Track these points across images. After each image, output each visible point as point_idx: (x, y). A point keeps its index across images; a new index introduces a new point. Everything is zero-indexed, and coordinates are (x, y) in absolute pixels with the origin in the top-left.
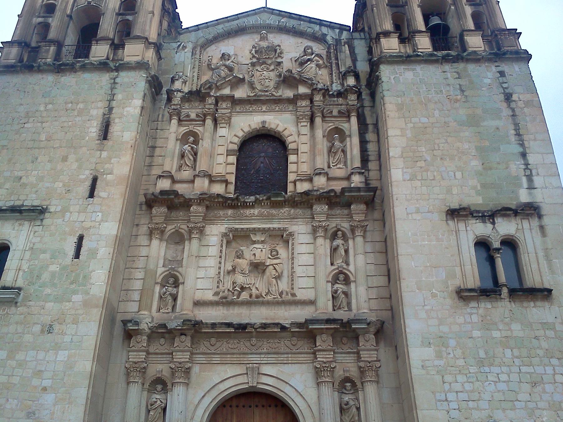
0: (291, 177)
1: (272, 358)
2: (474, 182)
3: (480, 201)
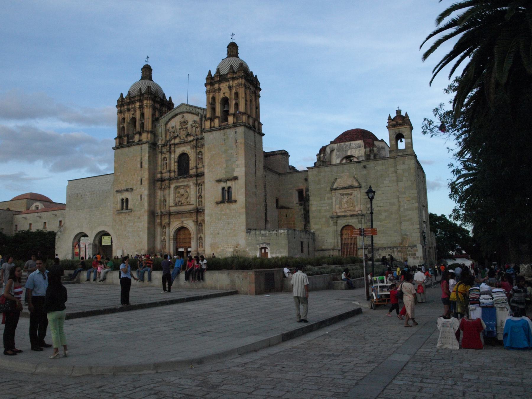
0: (190, 168)
1: (185, 219)
2: (224, 171)
3: (224, 176)
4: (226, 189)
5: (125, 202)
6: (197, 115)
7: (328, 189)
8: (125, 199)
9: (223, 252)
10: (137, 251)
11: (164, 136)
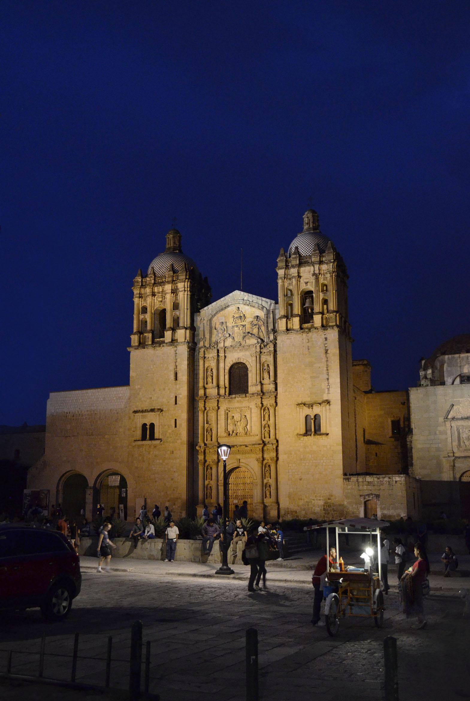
0: (250, 384)
3: (309, 400)
4: (313, 417)
7: (441, 419)
8: (148, 424)
9: (308, 505)
10: (169, 501)
11: (207, 336)
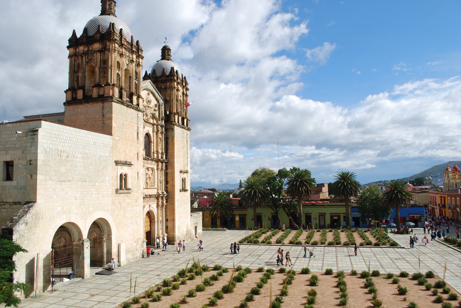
0: (152, 151)
5: (123, 178)
6: (158, 101)
10: (135, 242)
